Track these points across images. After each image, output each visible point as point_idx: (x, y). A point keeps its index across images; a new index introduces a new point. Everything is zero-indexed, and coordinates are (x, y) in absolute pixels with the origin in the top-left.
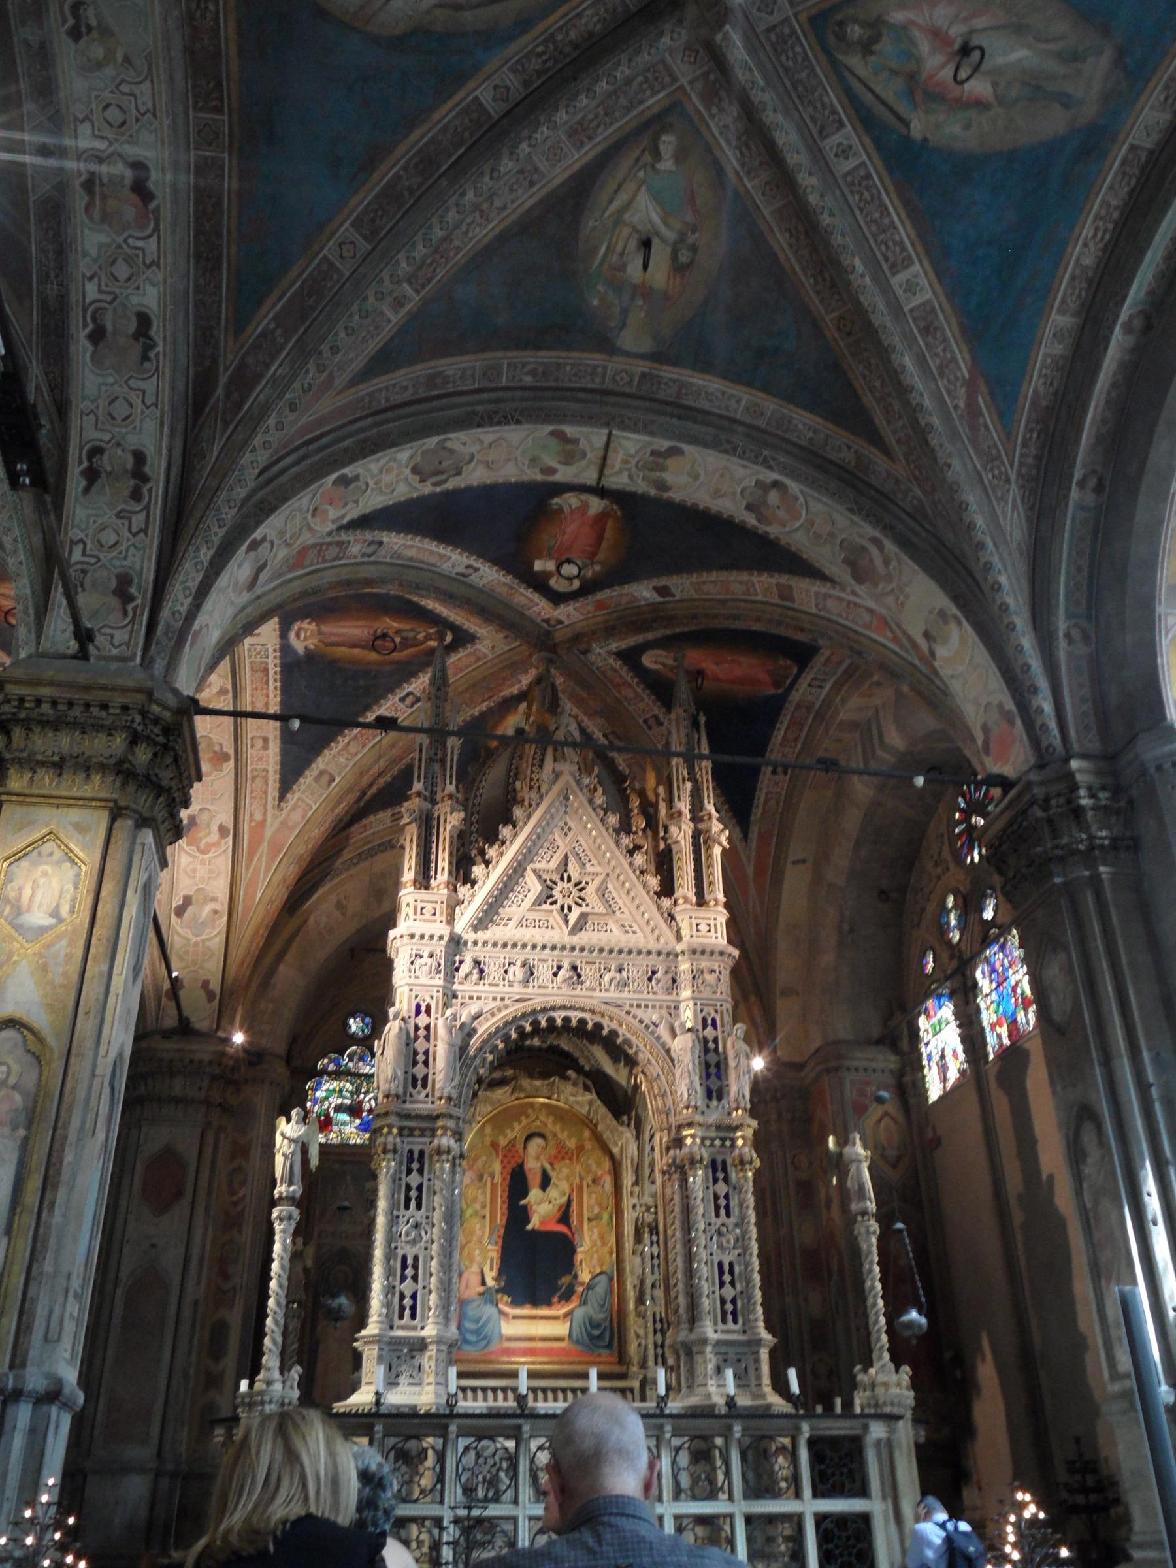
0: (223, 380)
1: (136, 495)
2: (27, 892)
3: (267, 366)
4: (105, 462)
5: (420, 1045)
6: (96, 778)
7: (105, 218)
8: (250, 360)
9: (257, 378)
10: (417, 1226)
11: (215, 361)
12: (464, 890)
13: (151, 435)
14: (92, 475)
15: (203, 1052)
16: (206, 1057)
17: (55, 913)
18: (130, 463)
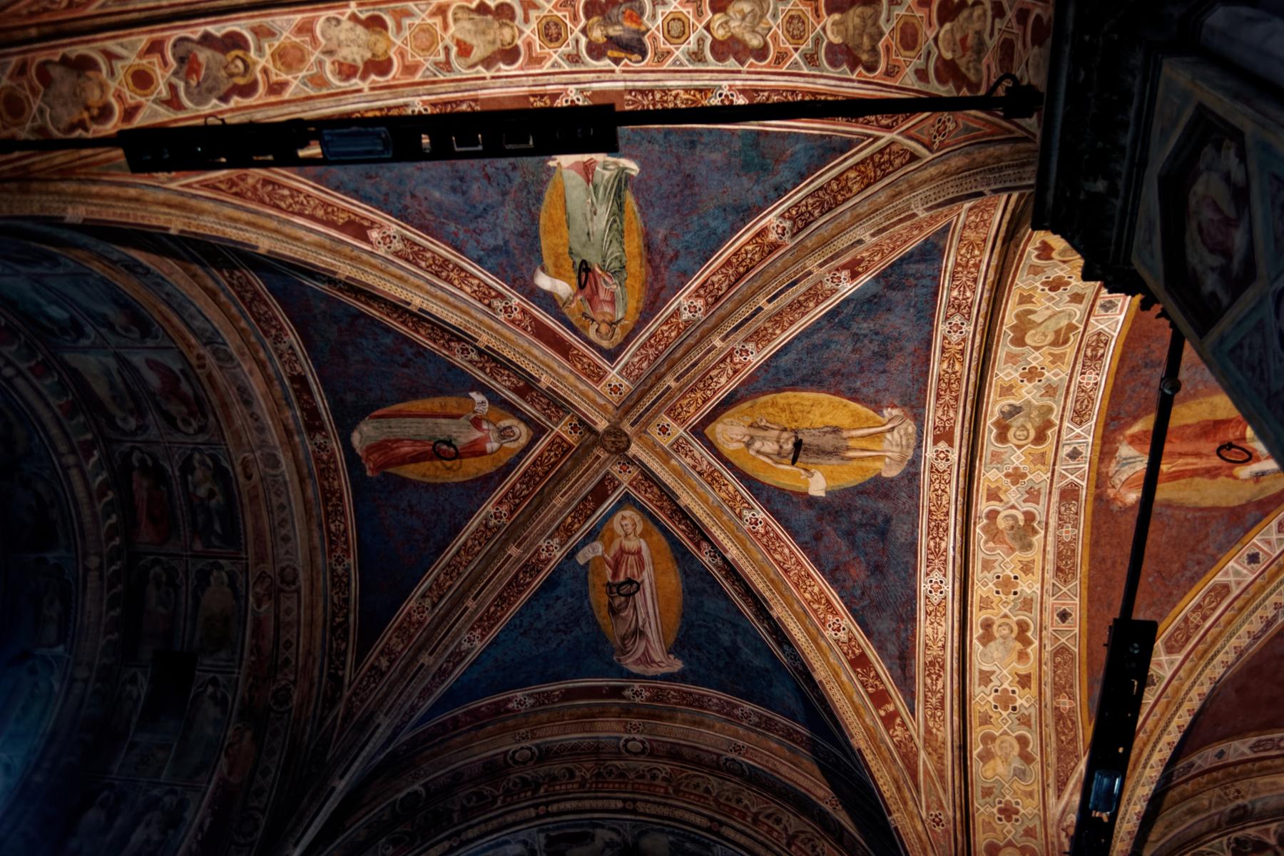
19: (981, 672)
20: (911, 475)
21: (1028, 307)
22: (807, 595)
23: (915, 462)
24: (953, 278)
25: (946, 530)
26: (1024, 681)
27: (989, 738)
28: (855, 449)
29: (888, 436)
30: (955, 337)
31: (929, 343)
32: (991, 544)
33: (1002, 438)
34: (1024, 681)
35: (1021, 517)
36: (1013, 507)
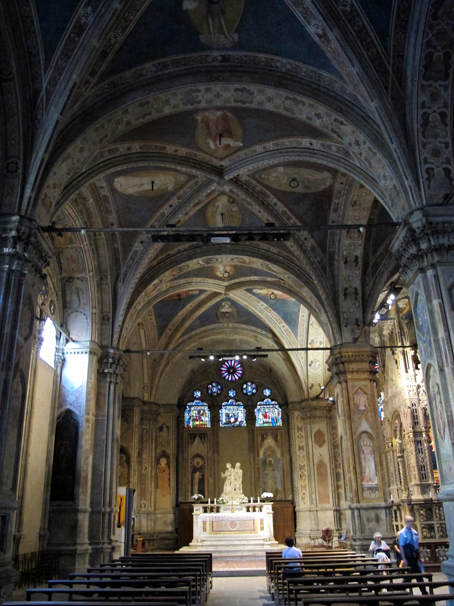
0: (371, 265)
1: (356, 299)
2: (358, 402)
3: (382, 261)
4: (348, 292)
5: (415, 414)
6: (366, 373)
7: (350, 237)
8: (378, 260)
9: (380, 264)
10: (422, 458)
11: (368, 261)
12: (417, 371)
13: (357, 283)
14: (345, 295)
15: (322, 403)
16: (324, 405)
17: (365, 406)
18: (354, 291)
19: (127, 110)
20: (203, 47)
21: (307, 105)
22: (127, 15)
23: (210, 48)
24: (313, 71)
25: (177, 67)
26: (128, 123)
27: (103, 126)
28: (213, 21)
29: (223, 36)
30: (279, 64)
31: (277, 54)
32: (184, 93)
33: (237, 90)
34: (128, 123)
35: (198, 100)
36: (203, 96)
